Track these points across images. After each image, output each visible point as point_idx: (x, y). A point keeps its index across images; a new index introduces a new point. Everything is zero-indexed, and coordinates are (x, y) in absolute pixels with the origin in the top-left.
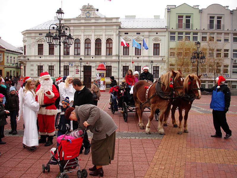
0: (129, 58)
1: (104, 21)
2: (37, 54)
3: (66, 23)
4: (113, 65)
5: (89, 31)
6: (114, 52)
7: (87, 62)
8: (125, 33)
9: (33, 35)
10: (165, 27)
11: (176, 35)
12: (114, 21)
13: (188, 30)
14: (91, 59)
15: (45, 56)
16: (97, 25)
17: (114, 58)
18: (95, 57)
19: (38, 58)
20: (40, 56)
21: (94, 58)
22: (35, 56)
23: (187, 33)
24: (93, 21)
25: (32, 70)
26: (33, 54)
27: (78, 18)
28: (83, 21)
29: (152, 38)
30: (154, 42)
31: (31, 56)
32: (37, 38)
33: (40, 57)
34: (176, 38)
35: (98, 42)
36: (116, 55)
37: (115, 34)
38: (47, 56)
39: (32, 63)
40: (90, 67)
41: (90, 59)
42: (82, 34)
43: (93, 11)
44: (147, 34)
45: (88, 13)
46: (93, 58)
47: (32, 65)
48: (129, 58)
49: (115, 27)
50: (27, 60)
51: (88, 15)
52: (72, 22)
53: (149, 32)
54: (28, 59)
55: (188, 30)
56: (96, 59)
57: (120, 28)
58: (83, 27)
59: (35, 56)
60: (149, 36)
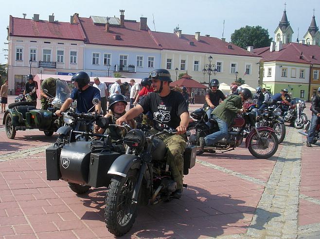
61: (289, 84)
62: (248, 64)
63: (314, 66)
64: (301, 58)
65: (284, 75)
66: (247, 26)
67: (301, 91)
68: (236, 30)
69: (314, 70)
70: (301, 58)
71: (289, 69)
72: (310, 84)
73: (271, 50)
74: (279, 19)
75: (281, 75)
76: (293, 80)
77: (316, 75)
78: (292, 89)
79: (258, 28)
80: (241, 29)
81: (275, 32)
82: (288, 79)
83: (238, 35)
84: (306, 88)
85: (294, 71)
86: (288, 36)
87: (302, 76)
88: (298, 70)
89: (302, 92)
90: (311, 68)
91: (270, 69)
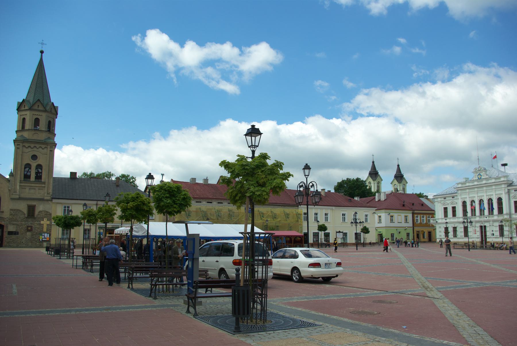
1: (493, 181)
2: (443, 217)
6: (505, 210)
9: (439, 199)
12: (502, 179)
14: (485, 219)
17: (506, 217)
19: (444, 221)
22: (442, 219)
24: (484, 182)
25: (440, 232)
26: (440, 217)
27: (473, 181)
28: (476, 183)
35: (490, 201)
36: (507, 214)
37: (503, 193)
39: (440, 225)
40: (485, 227)
42: (476, 196)
47: (440, 227)
49: (503, 186)
51: (480, 177)
52: (467, 184)
54: (437, 222)
59: (442, 219)
62: (367, 213)
63: (415, 212)
64: (404, 205)
65: (392, 221)
66: (347, 179)
68: (18, 102)
69: (415, 216)
70: (404, 205)
72: (413, 227)
73: (377, 200)
76: (400, 225)
78: (400, 233)
79: (358, 179)
80: (343, 181)
82: (396, 224)
83: (341, 186)
84: (410, 231)
85: (399, 217)
86: (378, 183)
87: (406, 221)
88: (403, 215)
89: (408, 235)
90: (413, 214)
91: (380, 217)
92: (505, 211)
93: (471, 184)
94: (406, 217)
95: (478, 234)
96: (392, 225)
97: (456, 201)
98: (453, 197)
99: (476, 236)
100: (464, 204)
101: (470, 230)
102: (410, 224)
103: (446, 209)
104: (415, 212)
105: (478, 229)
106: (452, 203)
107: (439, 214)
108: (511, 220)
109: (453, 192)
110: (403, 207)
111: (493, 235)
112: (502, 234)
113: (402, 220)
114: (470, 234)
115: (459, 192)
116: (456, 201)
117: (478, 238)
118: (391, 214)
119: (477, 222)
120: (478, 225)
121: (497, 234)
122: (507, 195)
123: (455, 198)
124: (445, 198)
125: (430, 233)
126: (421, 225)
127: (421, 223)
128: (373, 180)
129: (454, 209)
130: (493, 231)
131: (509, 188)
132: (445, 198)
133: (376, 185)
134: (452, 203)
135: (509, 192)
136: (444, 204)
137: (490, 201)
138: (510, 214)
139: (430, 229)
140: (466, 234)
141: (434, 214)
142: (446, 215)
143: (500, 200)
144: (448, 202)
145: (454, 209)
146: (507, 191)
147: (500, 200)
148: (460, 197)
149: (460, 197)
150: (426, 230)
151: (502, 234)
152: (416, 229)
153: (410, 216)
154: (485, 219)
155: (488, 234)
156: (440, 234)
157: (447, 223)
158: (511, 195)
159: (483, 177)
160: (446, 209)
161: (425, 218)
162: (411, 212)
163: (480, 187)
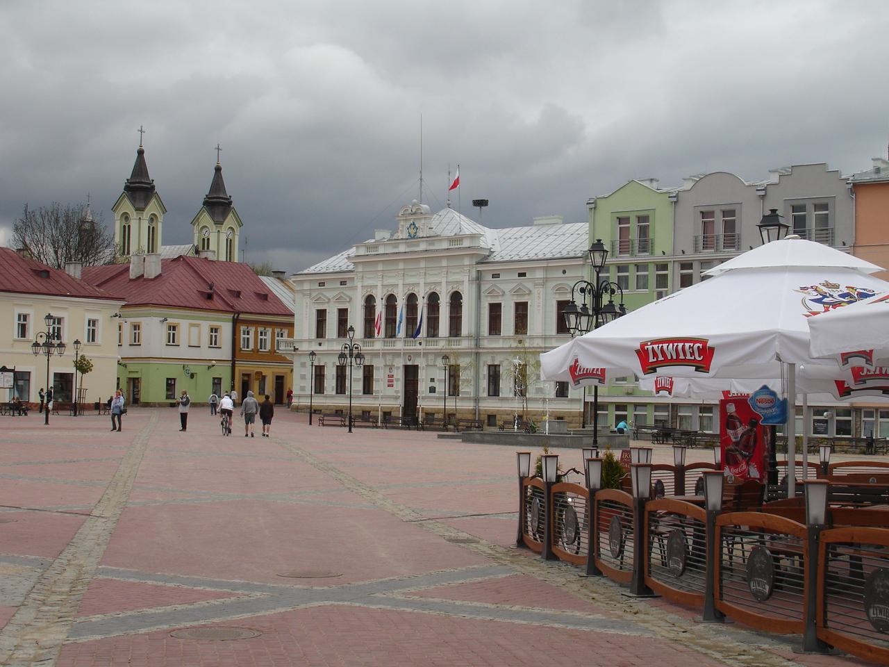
0: (500, 344)
1: (445, 245)
2: (314, 336)
3: (368, 253)
4: (463, 362)
5: (414, 273)
6: (467, 326)
7: (409, 355)
8: (494, 276)
9: (306, 286)
10: (580, 255)
11: (632, 274)
12: (466, 243)
13: (643, 258)
15: (329, 341)
16: (432, 257)
18: (427, 341)
19: (315, 347)
20: (320, 340)
21: (423, 344)
23: (638, 267)
24: (423, 247)
25: (303, 377)
26: (306, 336)
28: (402, 248)
29: (551, 284)
30: (489, 299)
31: (301, 341)
32: (314, 294)
33: (320, 344)
34: (632, 282)
36: (469, 337)
37: (466, 279)
38: (332, 340)
40: (416, 367)
41: (414, 347)
43: (423, 221)
44: (540, 274)
45: (413, 226)
46: (420, 344)
48: (500, 344)
49: (467, 261)
50: (291, 350)
51: (412, 231)
52: (381, 250)
53: (546, 269)
54: (296, 349)
55: (643, 258)
56: (428, 347)
57: (484, 260)
58: (402, 264)
59: (310, 341)
60: (546, 280)
61: (186, 363)
62: (93, 316)
63: (242, 316)
65: (172, 340)
67: (174, 379)
69: (243, 328)
71: (184, 325)
74: (126, 171)
75: (165, 340)
76: (193, 354)
77: (248, 339)
78: (192, 376)
81: (114, 208)
82: (183, 352)
84: (224, 373)
85: (194, 330)
86: (152, 220)
87: (214, 343)
88: (205, 326)
89: (217, 382)
90: (236, 322)
91: (136, 327)
92: (465, 330)
93: (390, 250)
94: (214, 330)
95: (399, 386)
96: (172, 352)
97: (348, 293)
98: (343, 283)
99: (390, 391)
100: (370, 301)
101: (377, 375)
102: (225, 352)
103: (321, 315)
104: (242, 316)
105: (399, 375)
106: (339, 299)
107: (305, 326)
108: (477, 354)
109: (344, 268)
110: (208, 299)
111: (432, 390)
112: (454, 391)
113: (200, 339)
114: (376, 386)
115: (360, 269)
116: (348, 293)
117: (397, 398)
118: (171, 321)
119: (396, 354)
120: (400, 363)
121: (441, 388)
122: (474, 288)
123: (348, 284)
124: (322, 284)
125: (280, 380)
126: (256, 355)
127: (256, 351)
128: (137, 209)
129: (343, 314)
130: (431, 376)
131: (481, 268)
132: (322, 284)
133: (145, 224)
134: (339, 299)
135: (479, 278)
136: (317, 301)
137: (433, 299)
138: (477, 338)
139: (280, 369)
140: (368, 389)
141: (291, 325)
142: (320, 333)
143: (456, 298)
144: (330, 295)
145: (343, 314)
146: (474, 275)
147: (456, 298)
148: (359, 285)
149: (359, 285)
150: (270, 371)
151: (454, 391)
152: (242, 367)
153: (226, 329)
154: (418, 347)
155: (423, 388)
156: (301, 383)
157: (313, 354)
158: (484, 287)
159: (420, 234)
160: (321, 315)
161: (268, 337)
162: (230, 316)
163: (411, 259)
